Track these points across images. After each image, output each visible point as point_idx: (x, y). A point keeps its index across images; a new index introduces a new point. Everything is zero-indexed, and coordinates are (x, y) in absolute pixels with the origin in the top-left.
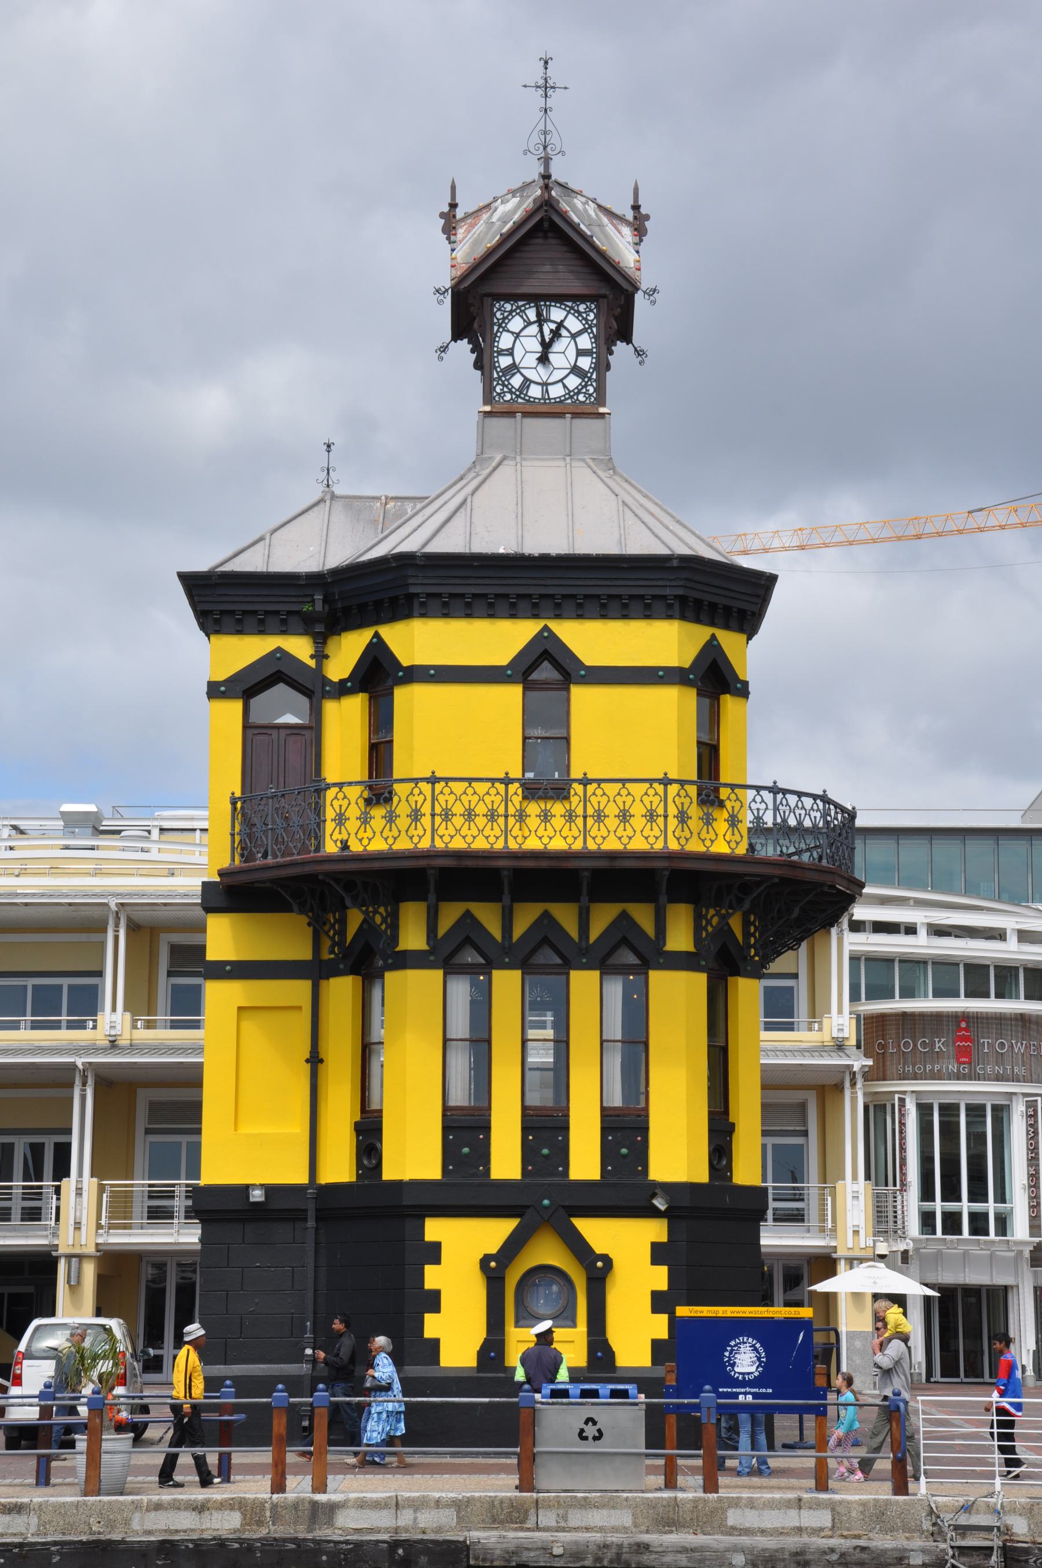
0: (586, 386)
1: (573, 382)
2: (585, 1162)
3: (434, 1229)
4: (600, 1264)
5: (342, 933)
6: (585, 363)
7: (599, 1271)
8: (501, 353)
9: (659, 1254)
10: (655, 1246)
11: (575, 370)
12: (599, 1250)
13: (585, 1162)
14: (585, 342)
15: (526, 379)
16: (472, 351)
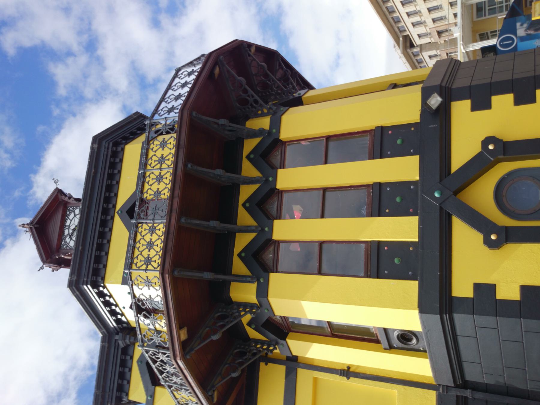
2: (404, 169)
3: (462, 288)
4: (491, 147)
5: (263, 343)
7: (497, 149)
9: (481, 103)
10: (474, 108)
12: (477, 149)
13: (404, 169)
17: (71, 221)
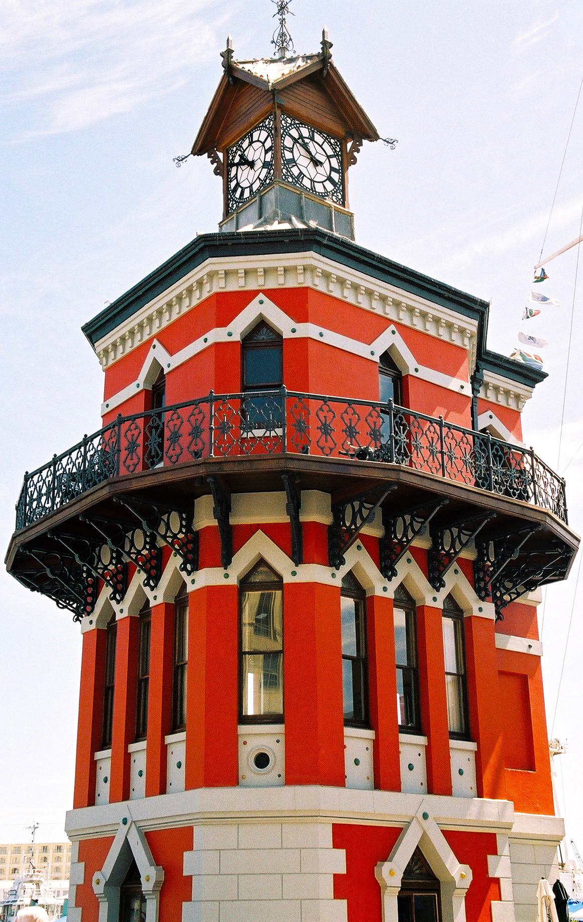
0: (336, 192)
1: (330, 187)
6: (336, 177)
8: (285, 147)
11: (330, 179)
14: (335, 163)
15: (301, 173)
16: (212, 163)
17: (321, 146)
